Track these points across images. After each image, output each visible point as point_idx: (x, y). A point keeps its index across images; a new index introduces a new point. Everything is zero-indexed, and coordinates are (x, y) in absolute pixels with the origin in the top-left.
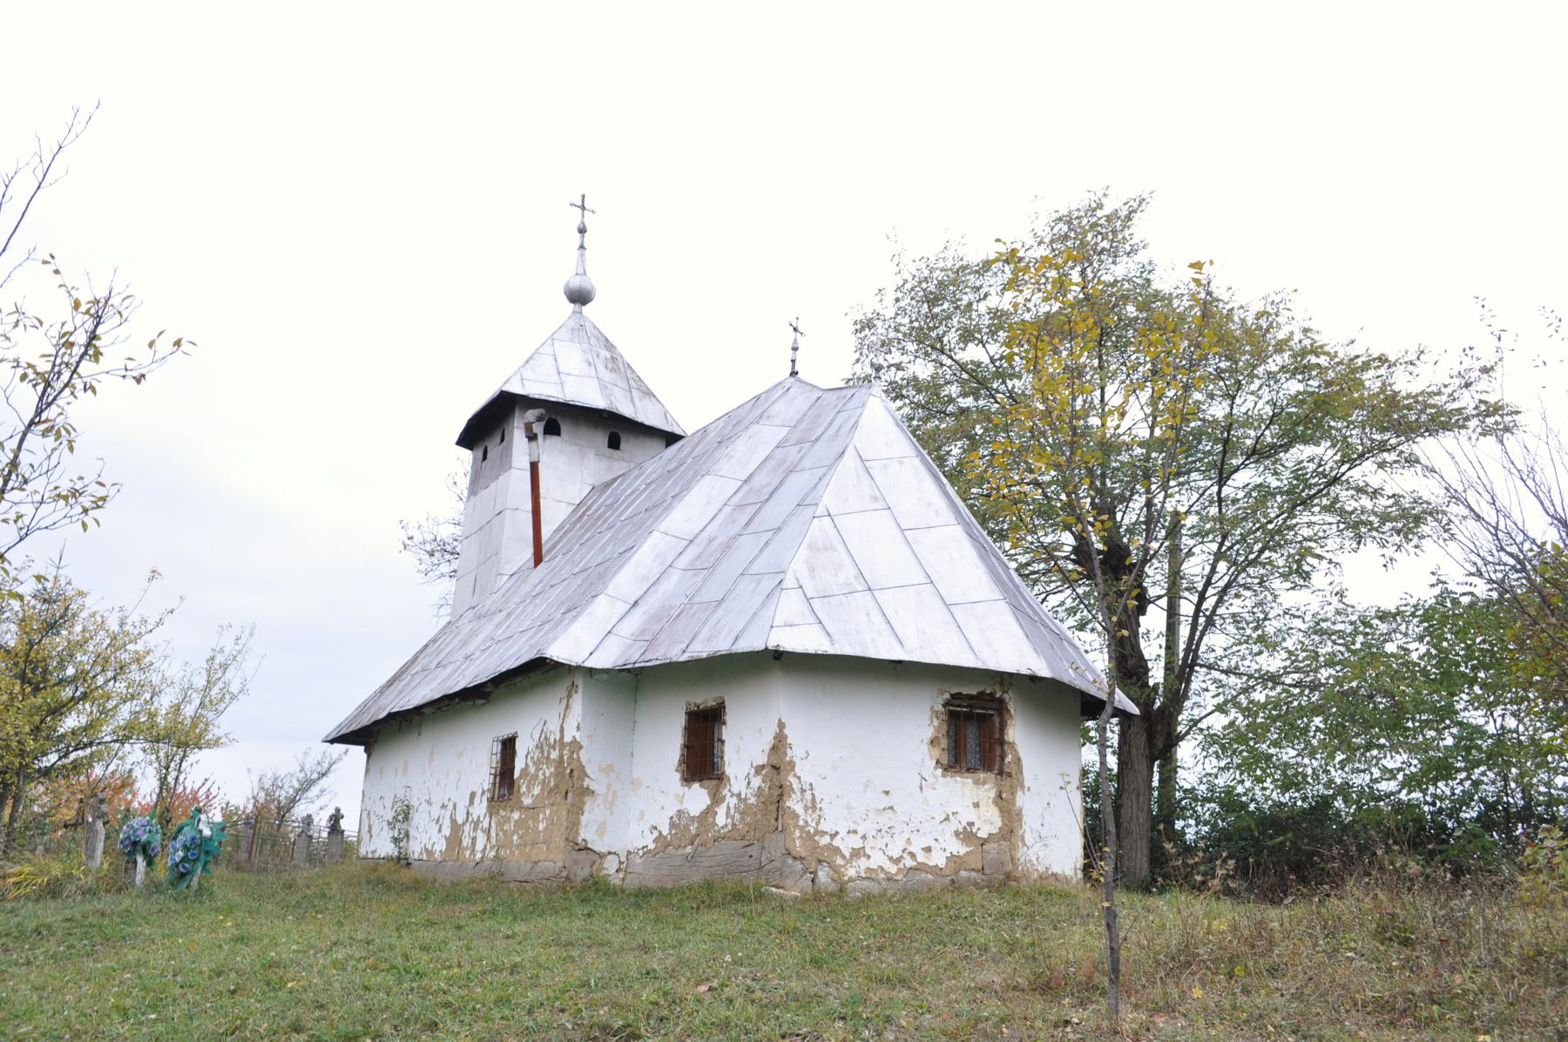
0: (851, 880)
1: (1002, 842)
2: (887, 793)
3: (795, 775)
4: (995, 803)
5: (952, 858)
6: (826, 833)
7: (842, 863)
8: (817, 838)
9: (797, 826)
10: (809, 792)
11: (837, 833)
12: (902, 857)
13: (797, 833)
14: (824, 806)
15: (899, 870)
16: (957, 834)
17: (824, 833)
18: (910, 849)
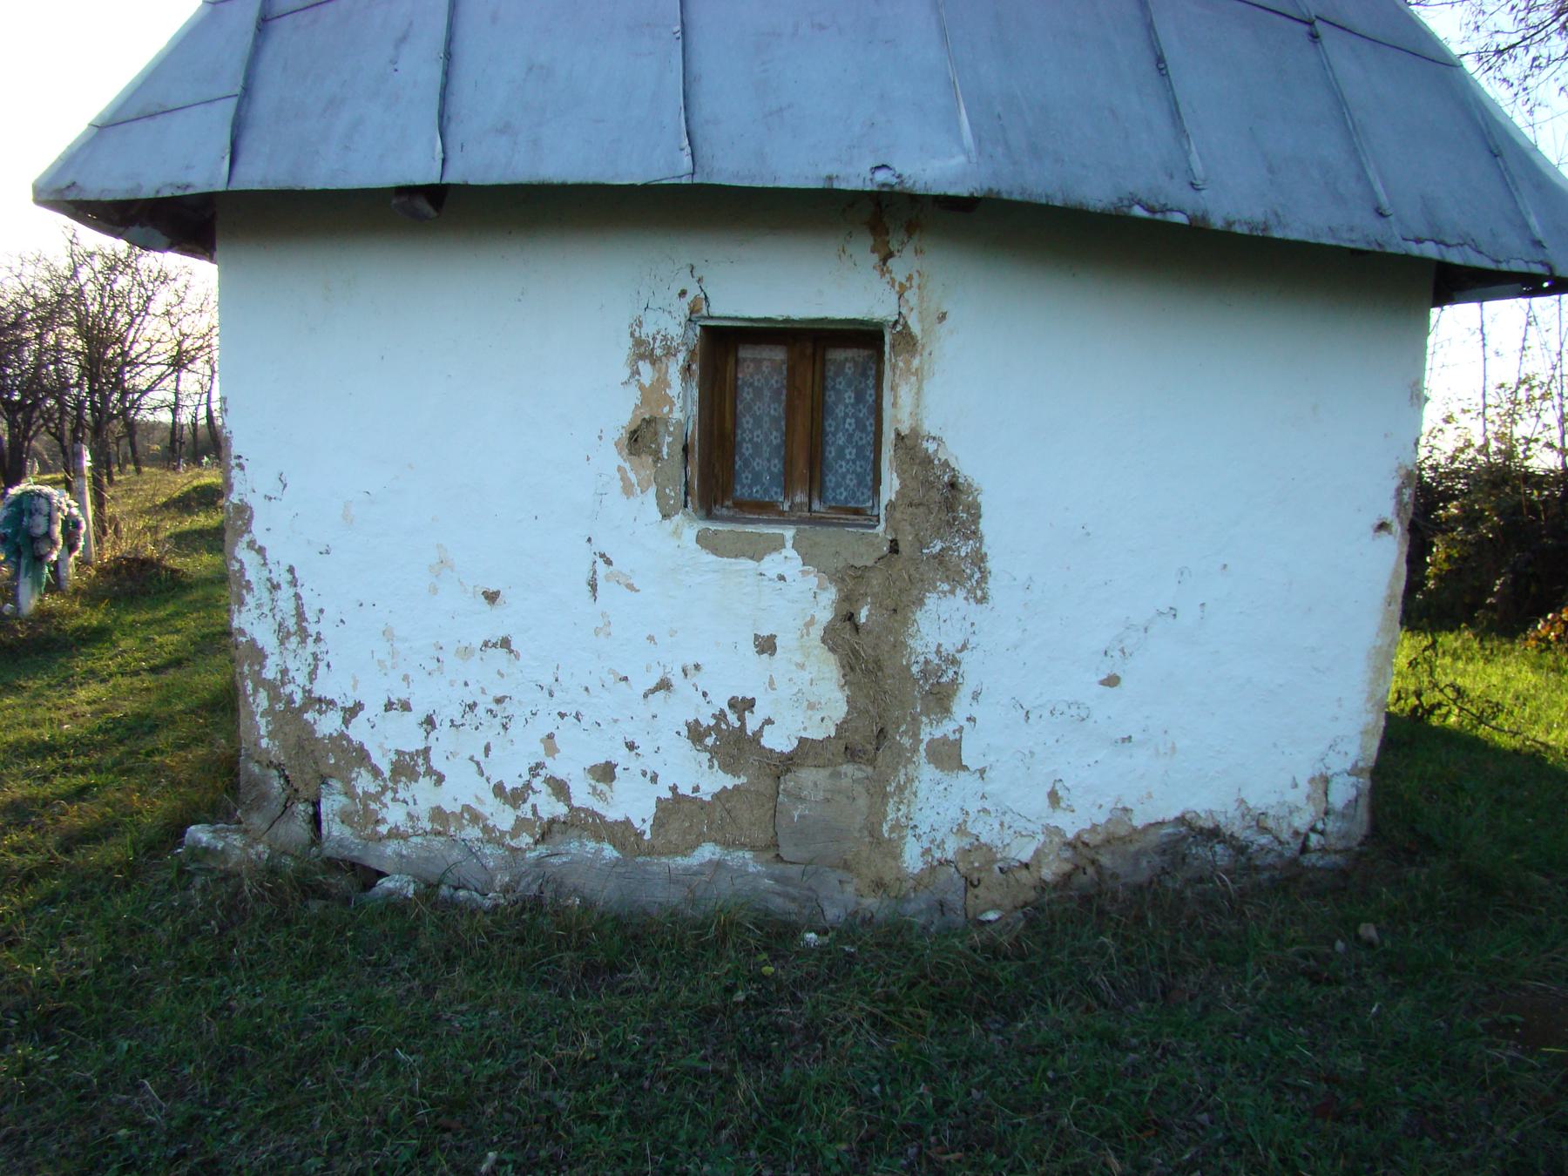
0: (395, 834)
1: (848, 769)
2: (492, 597)
3: (251, 545)
4: (831, 638)
5: (674, 807)
6: (332, 703)
7: (373, 788)
8: (309, 716)
9: (260, 682)
10: (286, 593)
11: (357, 708)
12: (528, 786)
13: (262, 700)
14: (326, 628)
15: (521, 825)
16: (696, 733)
17: (324, 704)
18: (556, 768)
